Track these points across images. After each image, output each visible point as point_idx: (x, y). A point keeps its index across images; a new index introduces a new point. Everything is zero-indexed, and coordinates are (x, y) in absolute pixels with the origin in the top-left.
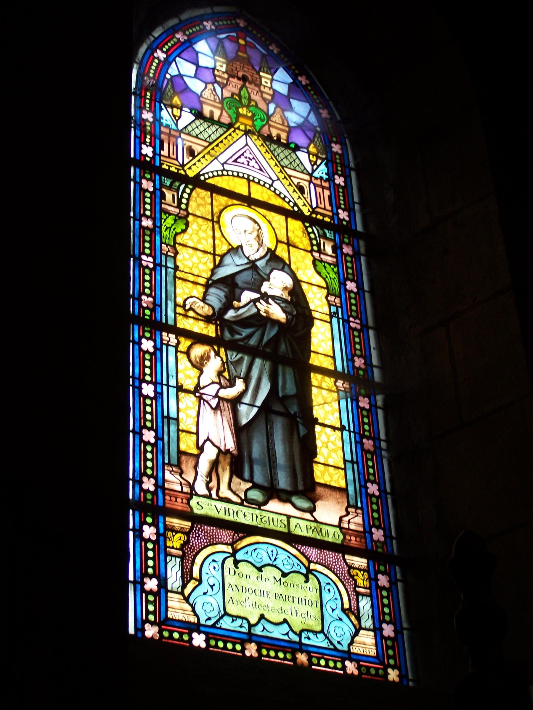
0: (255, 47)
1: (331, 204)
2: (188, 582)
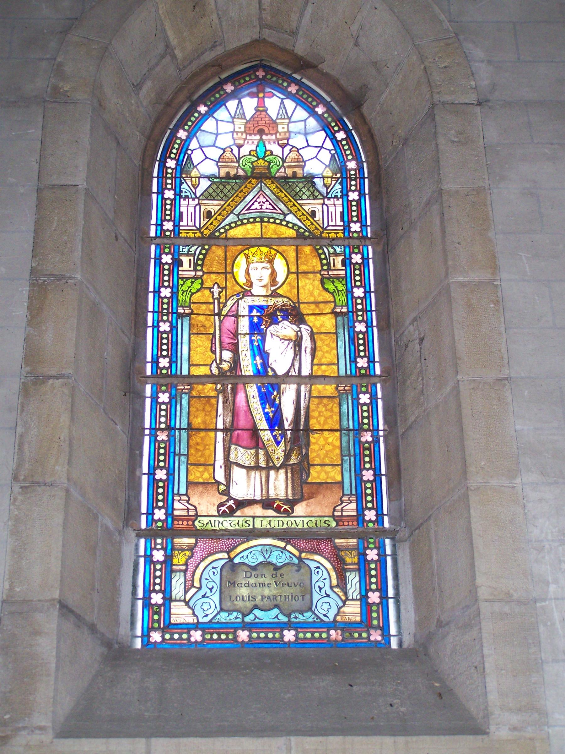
0: (274, 95)
1: (342, 219)
2: (189, 589)
